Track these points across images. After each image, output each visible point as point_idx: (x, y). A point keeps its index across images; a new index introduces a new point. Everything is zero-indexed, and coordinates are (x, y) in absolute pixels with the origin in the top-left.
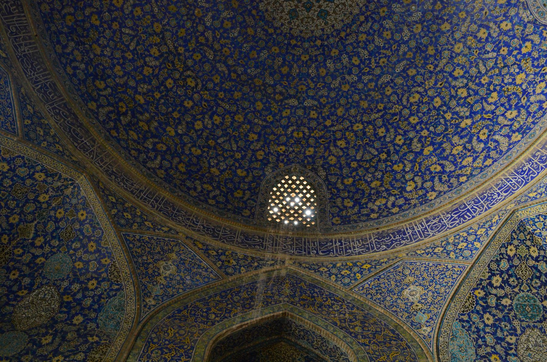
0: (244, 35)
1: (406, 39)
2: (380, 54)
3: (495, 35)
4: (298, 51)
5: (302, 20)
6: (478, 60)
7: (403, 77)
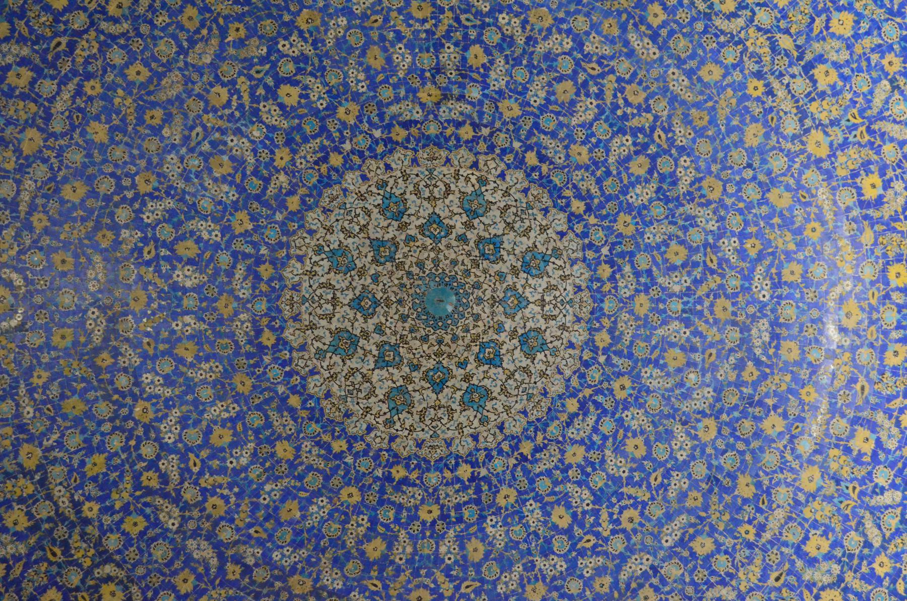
1: (682, 456)
2: (620, 497)
3: (892, 445)
4: (410, 497)
5: (422, 414)
6: (861, 512)
7: (681, 559)
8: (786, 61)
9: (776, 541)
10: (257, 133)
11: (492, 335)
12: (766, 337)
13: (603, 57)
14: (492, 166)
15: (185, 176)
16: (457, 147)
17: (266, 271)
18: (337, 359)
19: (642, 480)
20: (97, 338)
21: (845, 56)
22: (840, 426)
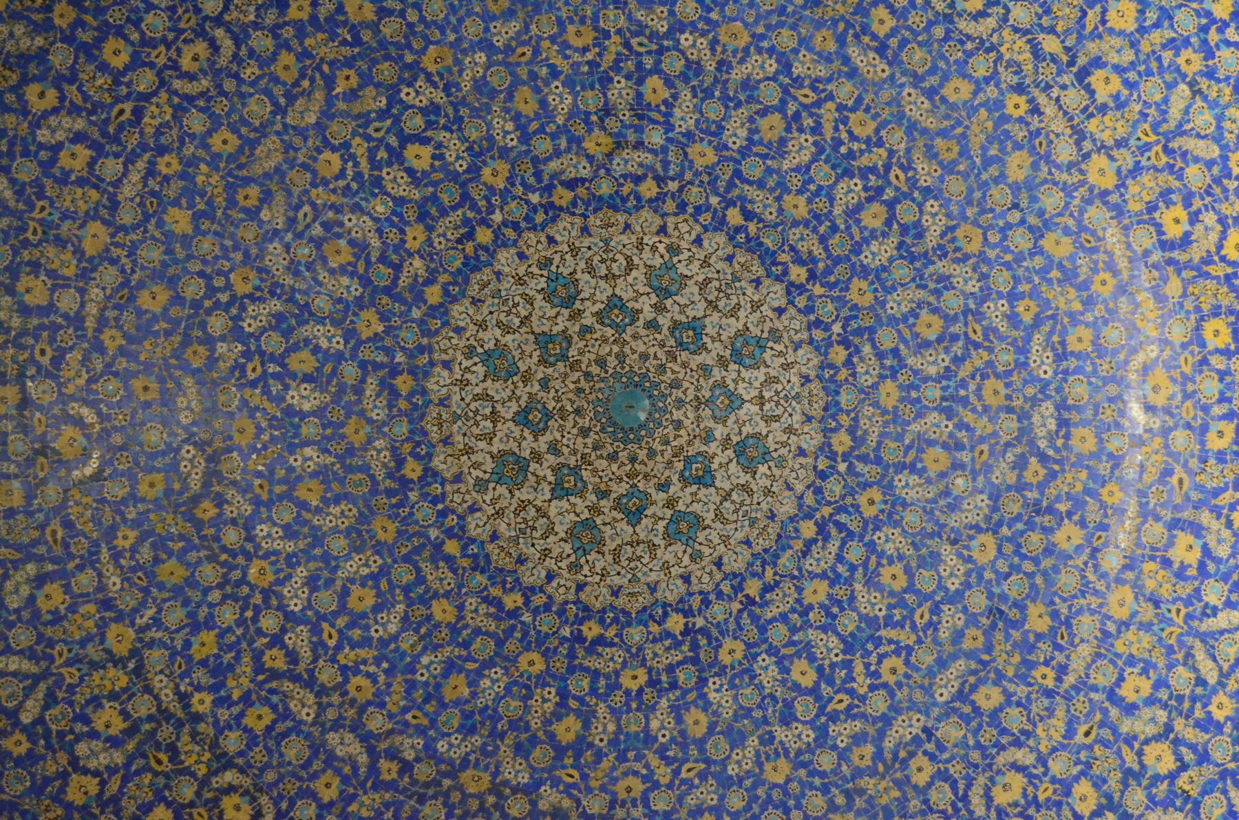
0: (420, 625)
1: (953, 585)
3: (1223, 551)
5: (616, 553)
6: (1189, 640)
7: (961, 717)
8: (1054, 68)
9: (1083, 685)
10: (381, 208)
11: (698, 446)
12: (1052, 425)
13: (817, 80)
14: (685, 229)
15: (293, 269)
16: (638, 208)
17: (403, 383)
18: (502, 490)
19: (904, 618)
20: (195, 484)
21: (1128, 56)
22: (1155, 532)
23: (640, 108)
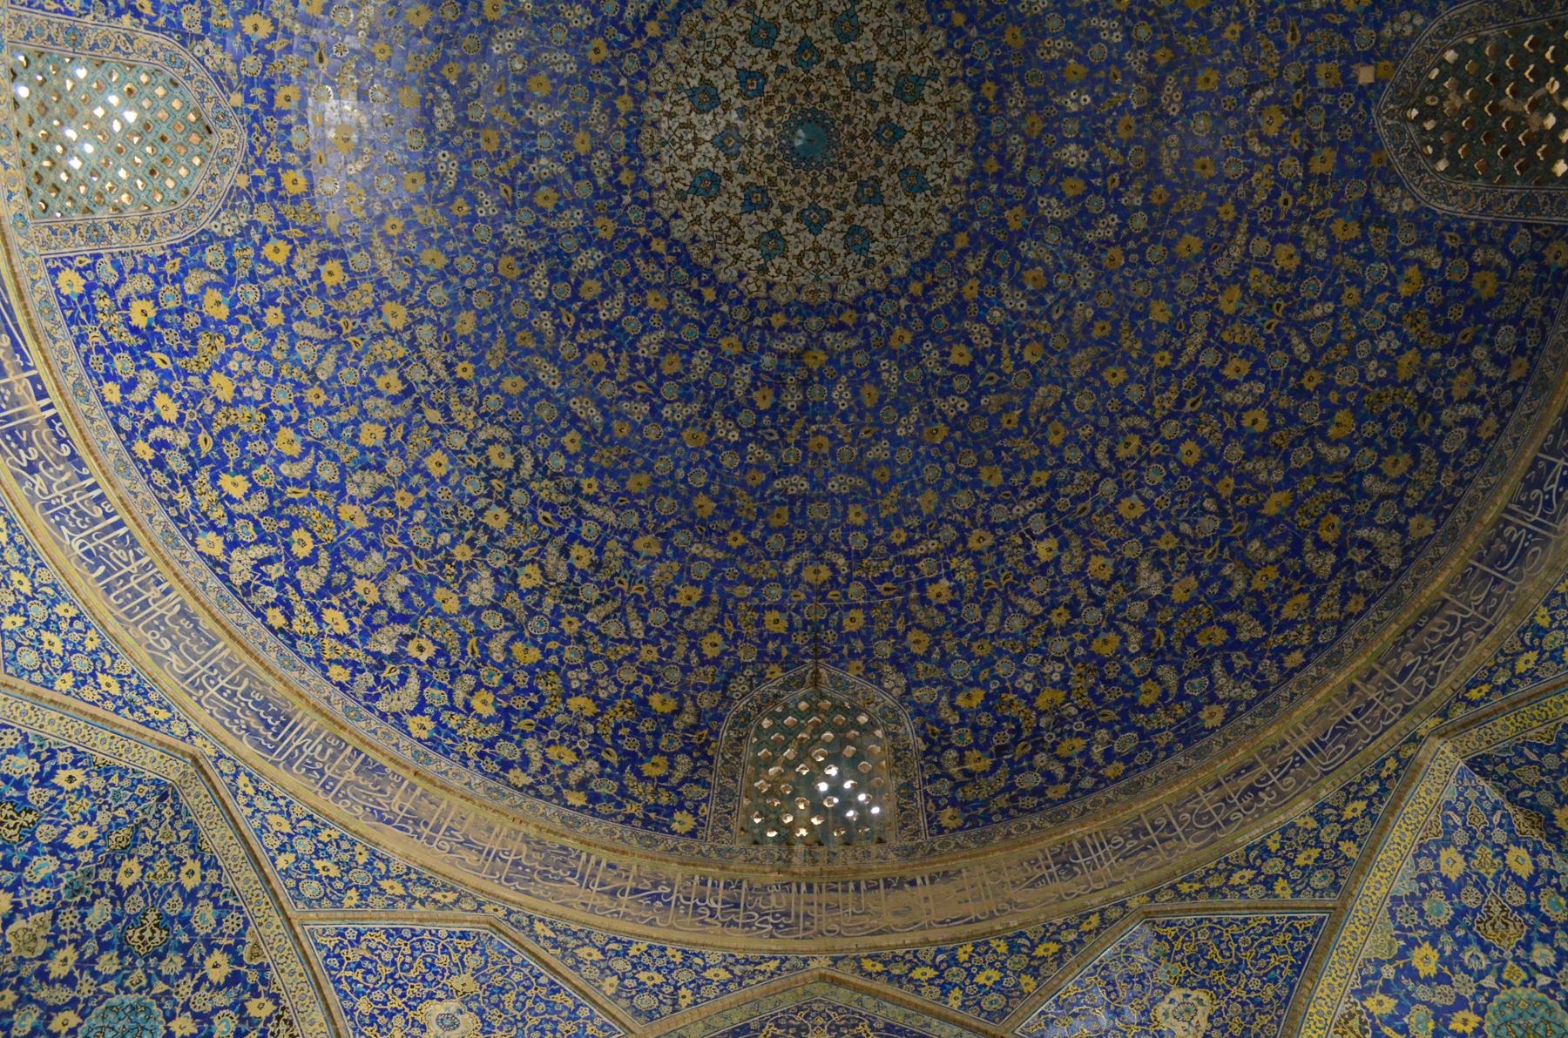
12: (437, 112)
13: (629, 399)
14: (751, 286)
15: (1073, 267)
16: (788, 305)
17: (992, 166)
20: (1171, 79)
21: (369, 404)
23: (778, 386)
